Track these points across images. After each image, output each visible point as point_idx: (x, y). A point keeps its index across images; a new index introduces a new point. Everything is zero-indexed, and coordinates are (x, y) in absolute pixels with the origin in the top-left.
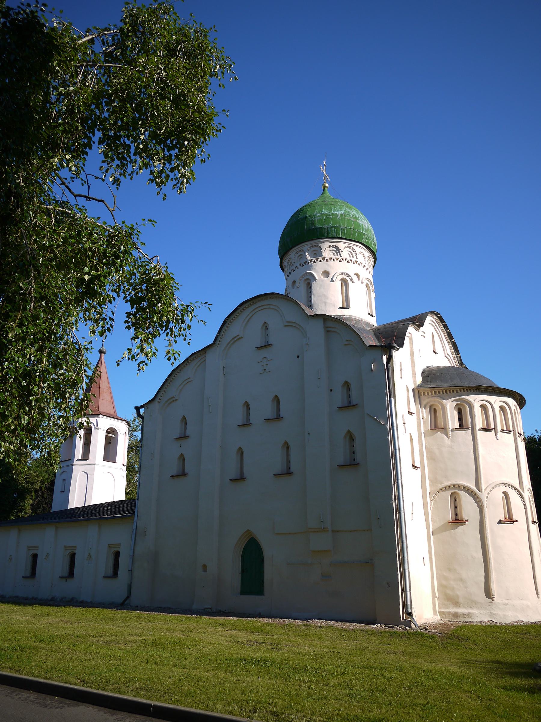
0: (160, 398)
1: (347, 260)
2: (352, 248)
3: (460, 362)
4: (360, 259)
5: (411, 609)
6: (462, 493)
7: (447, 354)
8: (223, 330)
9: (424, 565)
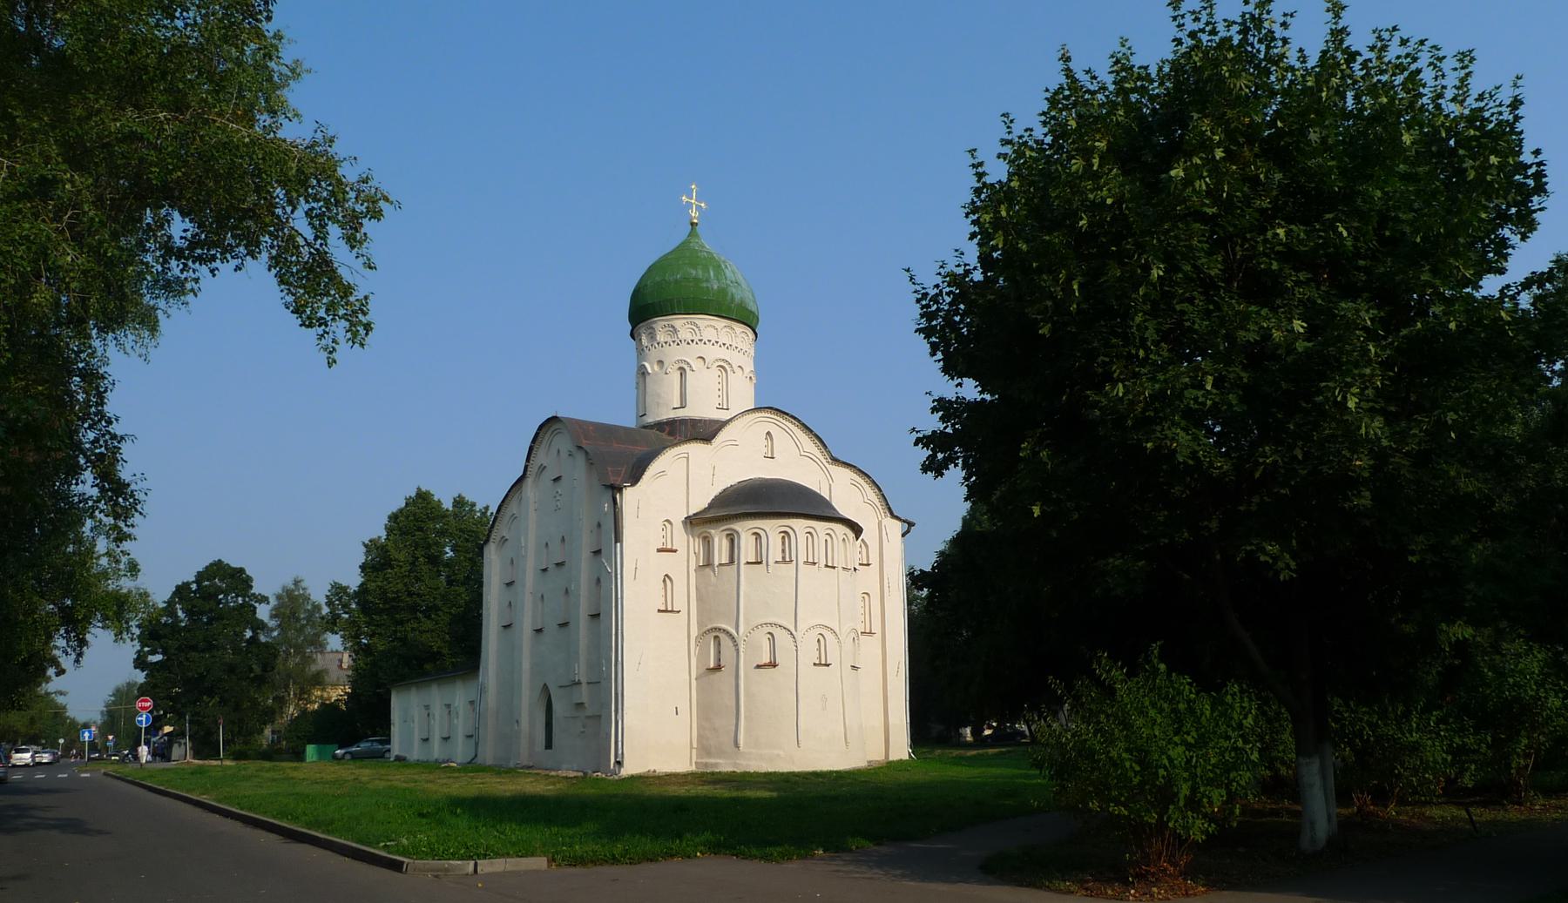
4: (709, 334)
5: (623, 757)
6: (722, 636)
8: (532, 458)
9: (677, 714)
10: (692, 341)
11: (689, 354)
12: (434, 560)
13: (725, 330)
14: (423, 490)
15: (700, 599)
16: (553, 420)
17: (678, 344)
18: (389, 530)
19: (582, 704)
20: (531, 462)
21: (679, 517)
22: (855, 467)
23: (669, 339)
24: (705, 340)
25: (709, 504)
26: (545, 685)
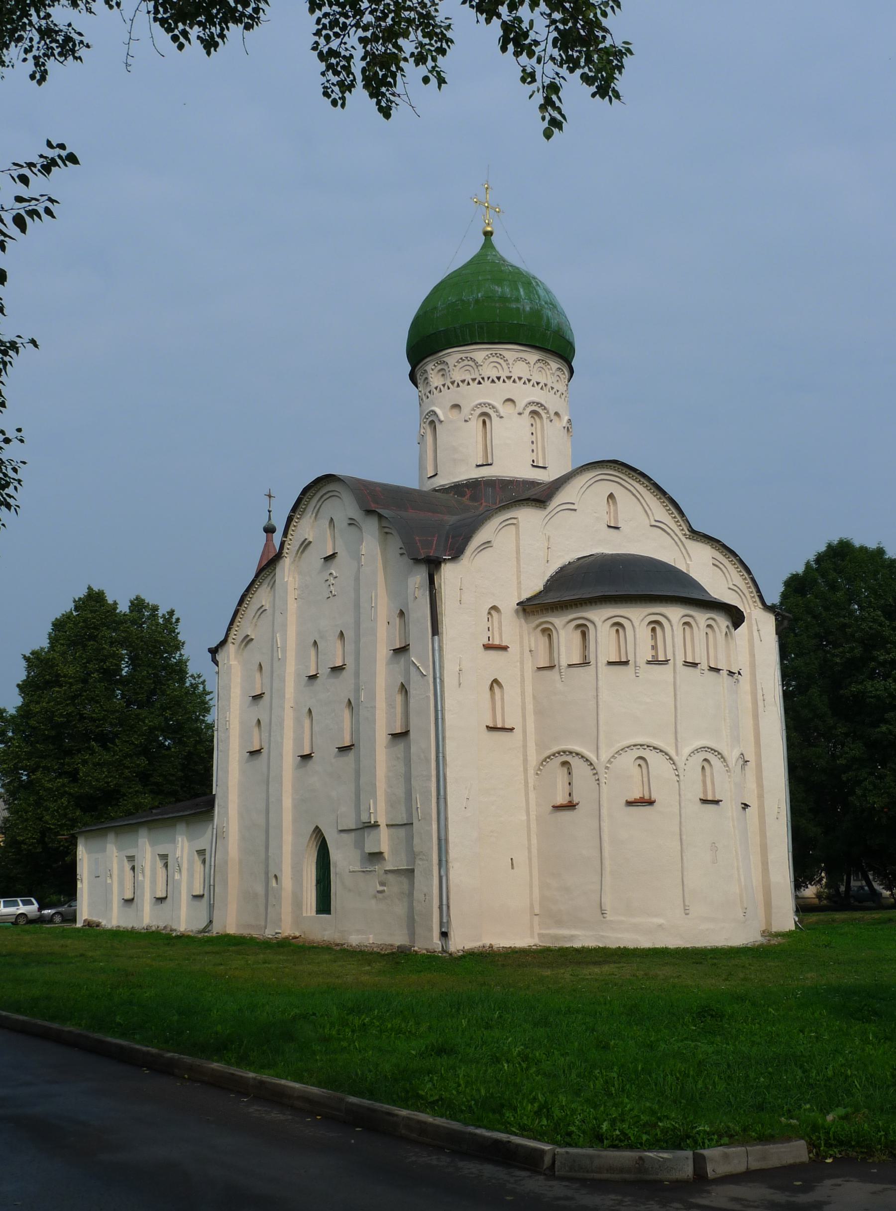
0: (234, 637)
1: (490, 379)
2: (500, 355)
3: (690, 529)
7: (656, 521)
8: (290, 532)
9: (513, 868)
10: (499, 378)
11: (494, 395)
12: (110, 675)
13: (539, 365)
14: (96, 589)
15: (539, 713)
16: (328, 479)
17: (480, 383)
18: (53, 640)
19: (381, 853)
20: (290, 537)
21: (509, 604)
22: (718, 541)
23: (468, 377)
24: (515, 377)
25: (545, 586)
26: (317, 827)
